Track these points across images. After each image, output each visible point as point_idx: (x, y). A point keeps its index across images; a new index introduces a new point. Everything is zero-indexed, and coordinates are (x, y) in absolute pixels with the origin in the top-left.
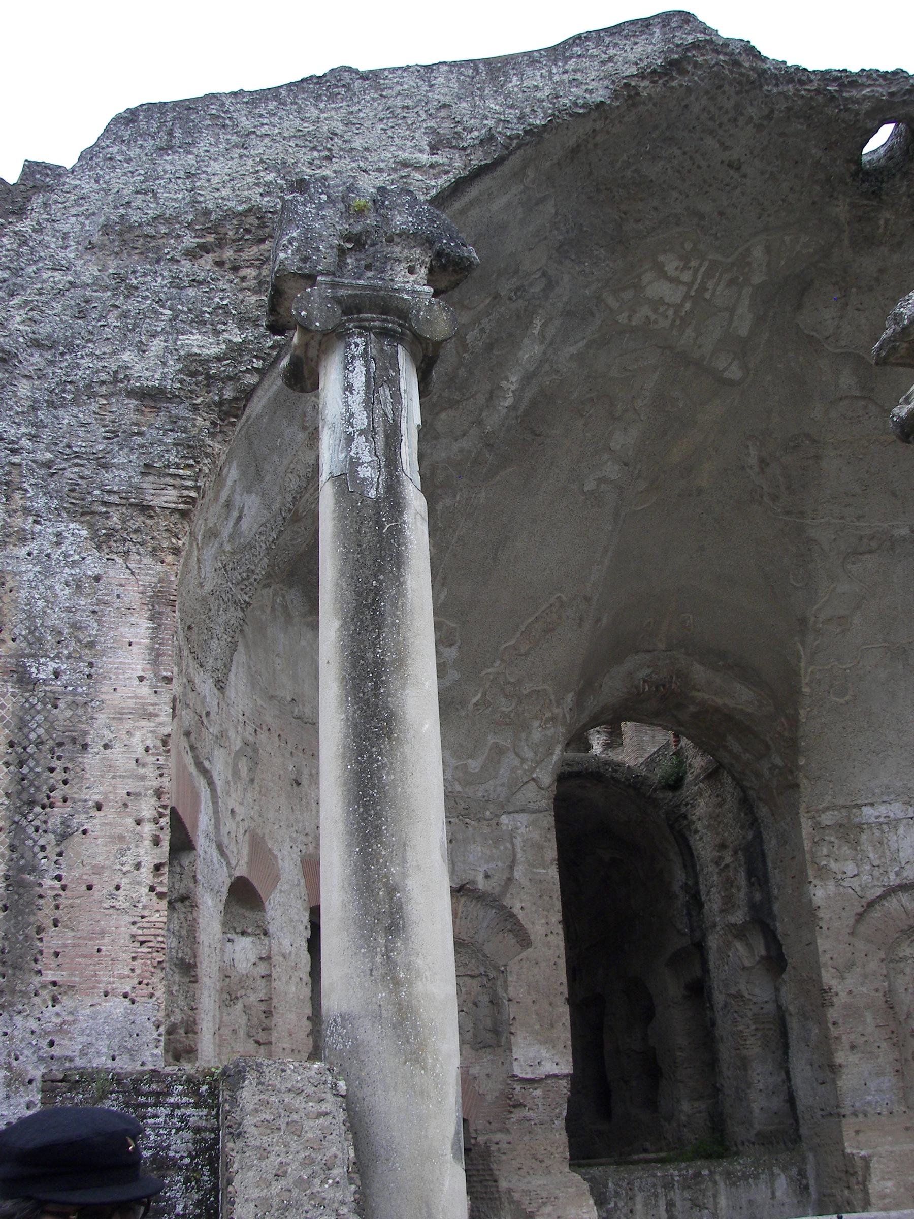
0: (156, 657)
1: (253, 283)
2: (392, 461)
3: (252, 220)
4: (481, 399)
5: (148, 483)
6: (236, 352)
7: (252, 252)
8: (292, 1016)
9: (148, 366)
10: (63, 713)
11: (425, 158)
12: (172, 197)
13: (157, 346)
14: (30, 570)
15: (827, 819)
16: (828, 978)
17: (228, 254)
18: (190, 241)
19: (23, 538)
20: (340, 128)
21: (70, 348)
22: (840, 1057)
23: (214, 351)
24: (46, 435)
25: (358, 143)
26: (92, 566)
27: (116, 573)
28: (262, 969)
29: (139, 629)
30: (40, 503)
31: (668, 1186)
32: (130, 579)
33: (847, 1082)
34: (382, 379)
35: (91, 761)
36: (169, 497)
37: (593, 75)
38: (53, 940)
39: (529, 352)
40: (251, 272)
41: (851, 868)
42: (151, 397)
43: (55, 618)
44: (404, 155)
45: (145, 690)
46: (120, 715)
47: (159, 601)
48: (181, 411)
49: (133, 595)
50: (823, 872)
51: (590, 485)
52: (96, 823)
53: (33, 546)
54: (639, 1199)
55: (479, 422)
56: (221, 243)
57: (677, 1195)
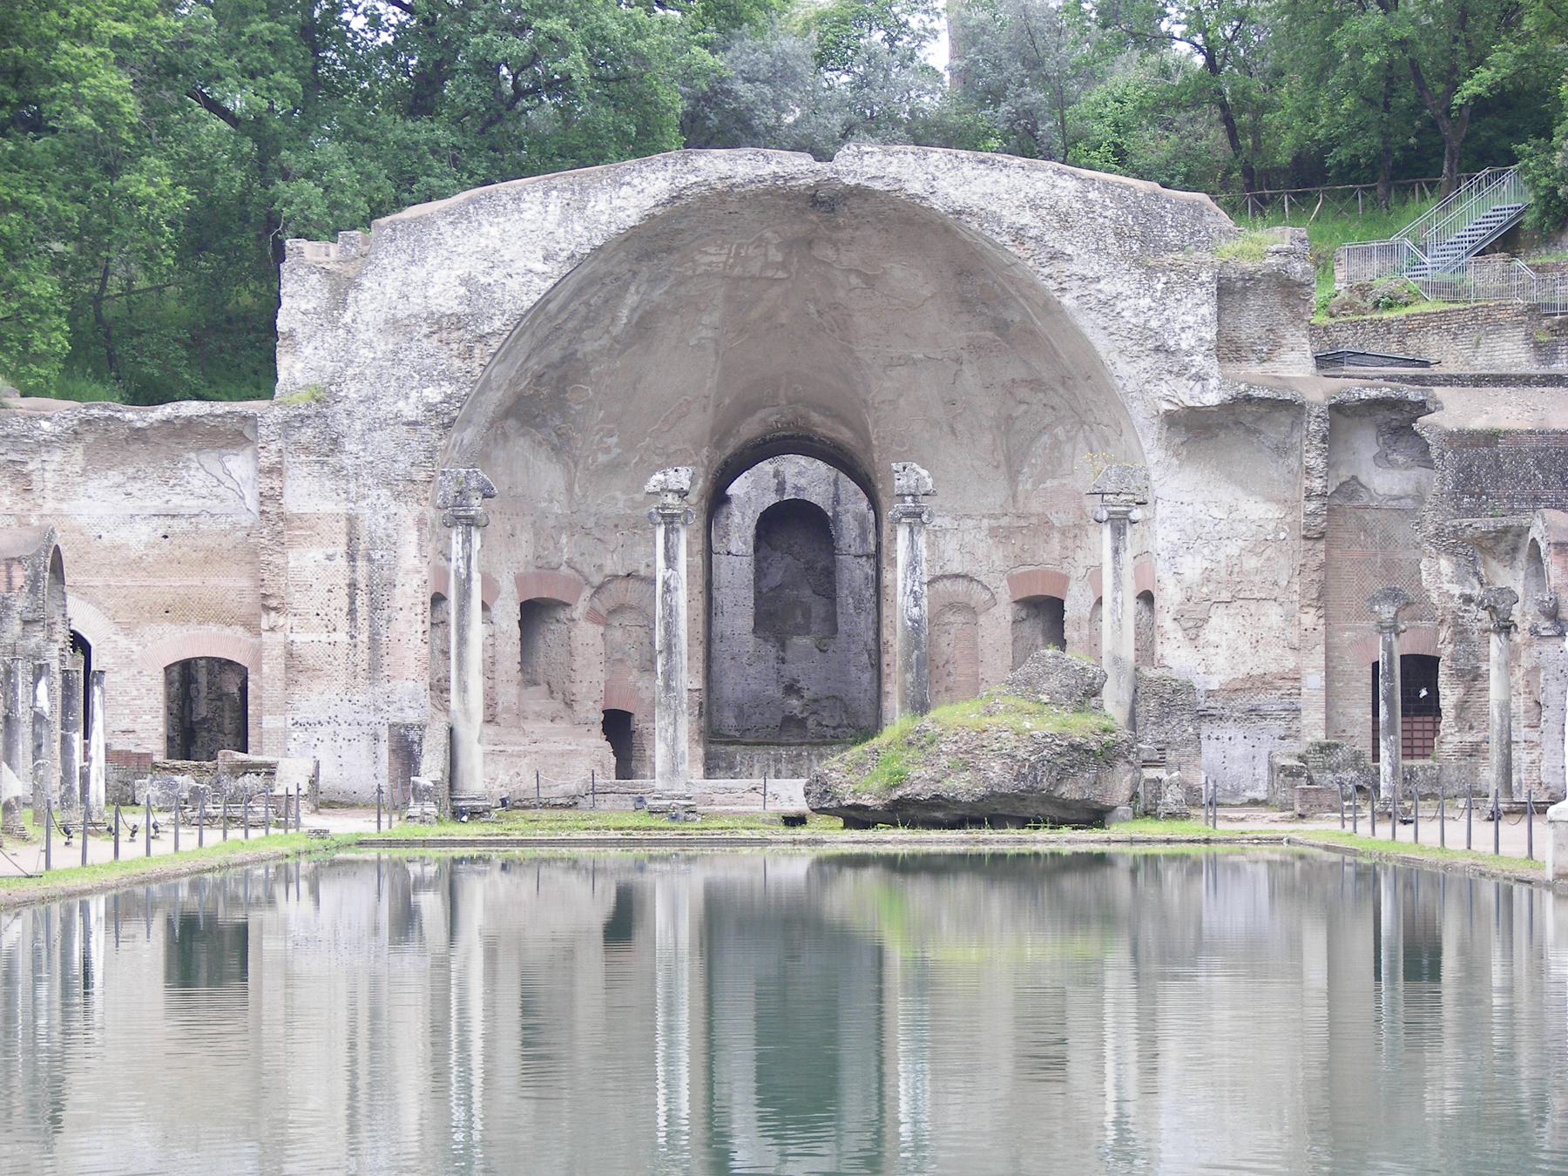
0: (421, 547)
1: (455, 353)
2: (469, 567)
3: (454, 319)
4: (607, 322)
5: (413, 470)
6: (448, 398)
7: (455, 335)
8: (508, 663)
9: (410, 410)
10: (386, 573)
11: (539, 267)
12: (416, 304)
13: (414, 394)
14: (368, 512)
17: (445, 334)
18: (425, 330)
20: (498, 245)
21: (375, 399)
23: (439, 398)
24: (370, 447)
25: (506, 258)
26: (393, 509)
27: (403, 511)
28: (490, 641)
29: (413, 536)
30: (370, 482)
31: (777, 760)
32: (408, 513)
34: (467, 540)
35: (397, 591)
36: (422, 476)
37: (633, 201)
38: (386, 660)
39: (632, 299)
40: (455, 346)
42: (413, 424)
43: (380, 532)
44: (530, 265)
45: (416, 562)
46: (407, 573)
47: (421, 522)
48: (425, 430)
49: (410, 521)
51: (693, 342)
52: (400, 615)
53: (368, 501)
54: (757, 767)
55: (608, 332)
56: (440, 329)
57: (783, 766)
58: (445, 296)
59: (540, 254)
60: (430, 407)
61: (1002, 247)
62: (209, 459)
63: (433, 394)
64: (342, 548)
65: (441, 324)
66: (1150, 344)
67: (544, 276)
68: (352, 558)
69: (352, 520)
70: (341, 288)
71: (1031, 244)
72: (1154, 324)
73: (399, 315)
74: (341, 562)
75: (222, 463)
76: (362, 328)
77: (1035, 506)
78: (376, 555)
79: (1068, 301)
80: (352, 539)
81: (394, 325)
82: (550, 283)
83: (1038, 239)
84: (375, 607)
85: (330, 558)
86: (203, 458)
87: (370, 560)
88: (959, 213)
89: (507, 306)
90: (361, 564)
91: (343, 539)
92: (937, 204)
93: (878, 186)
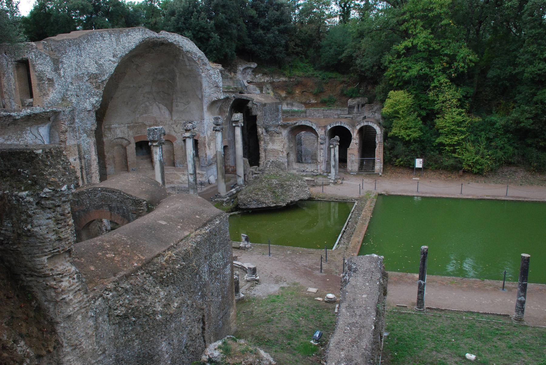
6: (97, 101)
9: (89, 107)
15: (106, 127)
16: (106, 154)
18: (87, 78)
19: (80, 137)
22: (107, 166)
33: (108, 170)
35: (92, 167)
41: (109, 135)
42: (90, 111)
50: (105, 136)
58: (93, 69)
59: (112, 55)
60: (93, 105)
61: (195, 61)
62: (34, 130)
63: (94, 100)
64: (77, 156)
65: (93, 77)
66: (215, 85)
67: (114, 62)
68: (80, 159)
69: (79, 146)
70: (57, 63)
71: (200, 61)
72: (217, 81)
73: (79, 73)
74: (78, 160)
75: (38, 131)
76: (67, 77)
77: (140, 120)
78: (86, 156)
79: (203, 75)
80: (79, 152)
81: (78, 78)
82: (116, 65)
83: (202, 60)
84: (87, 174)
85: (75, 160)
86: (33, 129)
87: (85, 158)
88: (187, 52)
89: (107, 71)
90: (83, 160)
91: (77, 153)
92: (184, 49)
93: (175, 43)
